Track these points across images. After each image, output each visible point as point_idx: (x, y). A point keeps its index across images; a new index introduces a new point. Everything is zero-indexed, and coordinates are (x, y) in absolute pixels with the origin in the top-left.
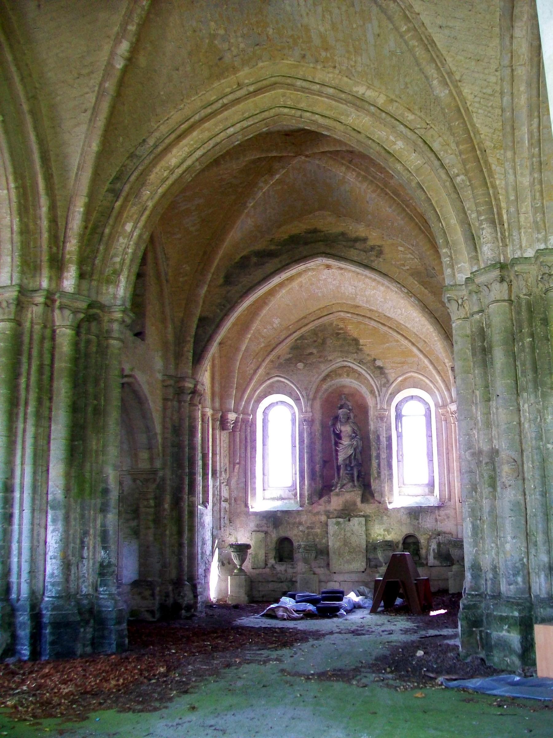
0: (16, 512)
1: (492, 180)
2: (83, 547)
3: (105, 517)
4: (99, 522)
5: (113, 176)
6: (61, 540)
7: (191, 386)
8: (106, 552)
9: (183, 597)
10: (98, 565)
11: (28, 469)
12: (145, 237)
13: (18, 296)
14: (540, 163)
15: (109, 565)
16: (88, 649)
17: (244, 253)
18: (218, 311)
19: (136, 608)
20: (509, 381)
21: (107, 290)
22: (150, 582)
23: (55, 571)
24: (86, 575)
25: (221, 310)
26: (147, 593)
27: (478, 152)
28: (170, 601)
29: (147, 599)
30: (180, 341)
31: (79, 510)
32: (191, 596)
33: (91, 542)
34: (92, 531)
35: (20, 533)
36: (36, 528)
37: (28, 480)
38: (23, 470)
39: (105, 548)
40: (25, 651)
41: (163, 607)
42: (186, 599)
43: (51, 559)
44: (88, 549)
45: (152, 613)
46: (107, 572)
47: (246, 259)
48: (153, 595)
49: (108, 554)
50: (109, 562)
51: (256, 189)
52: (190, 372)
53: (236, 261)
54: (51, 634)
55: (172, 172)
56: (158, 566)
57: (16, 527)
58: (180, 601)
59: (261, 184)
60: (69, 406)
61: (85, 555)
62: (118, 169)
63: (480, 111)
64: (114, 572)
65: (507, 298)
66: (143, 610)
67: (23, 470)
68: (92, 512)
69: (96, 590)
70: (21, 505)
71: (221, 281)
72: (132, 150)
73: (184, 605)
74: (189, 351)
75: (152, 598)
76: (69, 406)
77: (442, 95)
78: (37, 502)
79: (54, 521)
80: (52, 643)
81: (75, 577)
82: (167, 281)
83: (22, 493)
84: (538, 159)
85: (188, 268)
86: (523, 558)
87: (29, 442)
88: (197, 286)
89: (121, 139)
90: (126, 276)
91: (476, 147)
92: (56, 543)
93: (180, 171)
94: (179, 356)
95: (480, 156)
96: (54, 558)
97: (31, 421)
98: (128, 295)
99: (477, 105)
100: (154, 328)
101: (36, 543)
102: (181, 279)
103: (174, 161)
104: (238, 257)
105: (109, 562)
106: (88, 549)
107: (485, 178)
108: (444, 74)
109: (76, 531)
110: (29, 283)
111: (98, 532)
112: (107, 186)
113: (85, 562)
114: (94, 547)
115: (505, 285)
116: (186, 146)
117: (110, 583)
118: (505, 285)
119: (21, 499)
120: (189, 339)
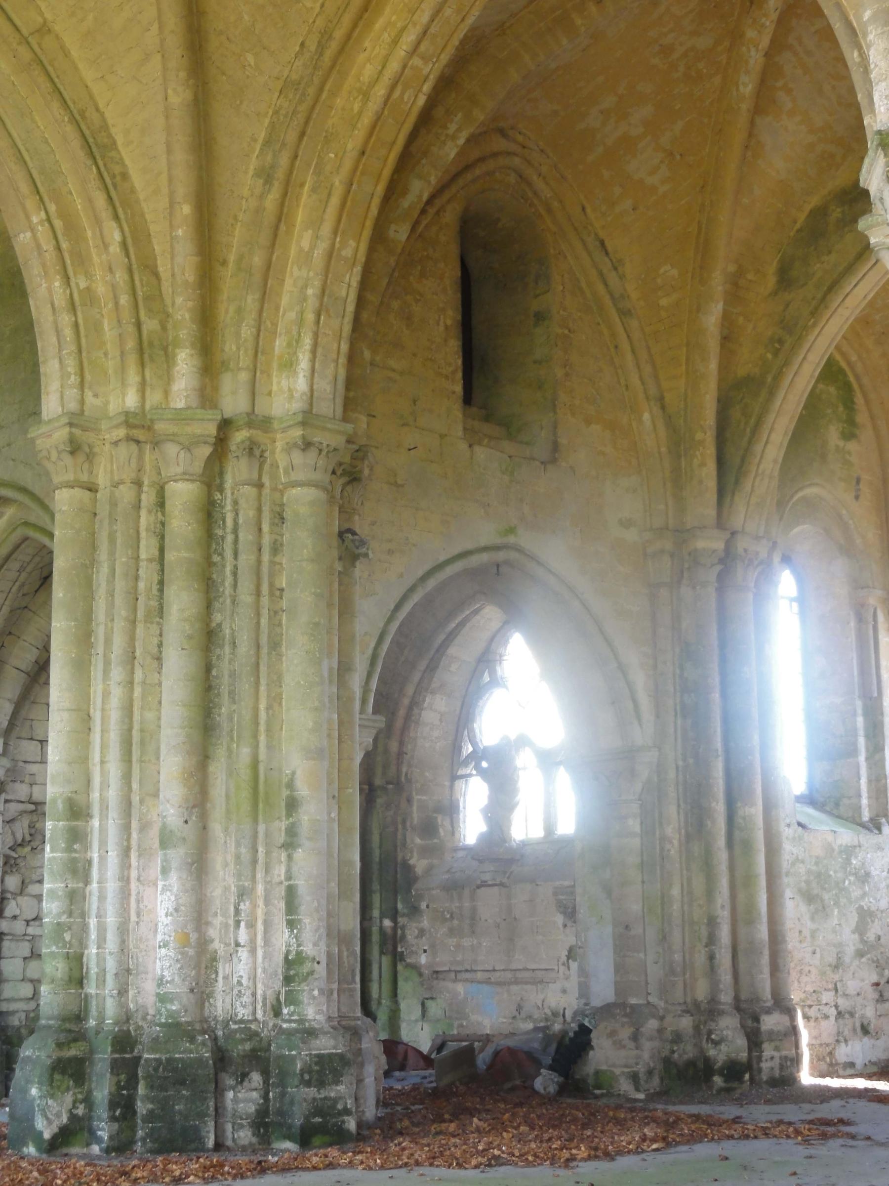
0: (95, 856)
2: (238, 923)
3: (290, 857)
4: (280, 871)
5: (260, 141)
6: (176, 910)
7: (720, 545)
8: (292, 931)
9: (716, 1043)
10: (279, 959)
11: (114, 770)
12: (348, 252)
13: (71, 433)
15: (300, 958)
16: (245, 1136)
17: (815, 201)
18: (769, 356)
19: (604, 1068)
21: (279, 383)
22: (632, 1007)
23: (166, 973)
24: (244, 981)
25: (776, 353)
26: (625, 1034)
28: (687, 1052)
29: (624, 1047)
30: (679, 445)
31: (232, 848)
32: (741, 1042)
33: (260, 913)
34: (260, 888)
35: (102, 898)
36: (134, 885)
37: (113, 794)
38: (104, 774)
39: (291, 924)
40: (104, 1131)
41: (667, 1062)
42: (723, 1047)
43: (160, 947)
44: (251, 925)
45: (634, 1078)
46: (296, 975)
47: (819, 213)
48: (635, 1037)
49: (296, 937)
50: (299, 953)
51: (744, 49)
52: (712, 512)
53: (798, 226)
54: (147, 1098)
55: (366, 96)
56: (655, 973)
57: (94, 886)
58: (712, 1053)
59: (750, 34)
60: (190, 637)
61: (243, 935)
62: (267, 121)
64: (312, 973)
66: (617, 1071)
67: (104, 774)
68: (261, 849)
69: (277, 1013)
70: (103, 843)
71: (772, 281)
72: (286, 74)
73: (719, 1064)
74: (703, 464)
75: (632, 1045)
76: (190, 637)
78: (135, 835)
79: (165, 871)
80: (151, 1117)
81: (225, 985)
82: (625, 313)
83: (103, 817)
85: (675, 272)
87: (115, 716)
88: (698, 310)
89: (250, 59)
90: (308, 347)
92: (167, 915)
93: (380, 91)
94: (678, 480)
96: (165, 946)
97: (117, 674)
98: (324, 385)
100: (596, 428)
101: (134, 918)
102: (664, 302)
103: (369, 71)
104: (802, 217)
105: (299, 953)
106: (251, 925)
109: (226, 889)
110: (108, 402)
111: (281, 891)
112: (253, 164)
113: (243, 954)
114: (267, 924)
116: (385, 29)
117: (305, 998)
119: (103, 830)
120: (699, 436)
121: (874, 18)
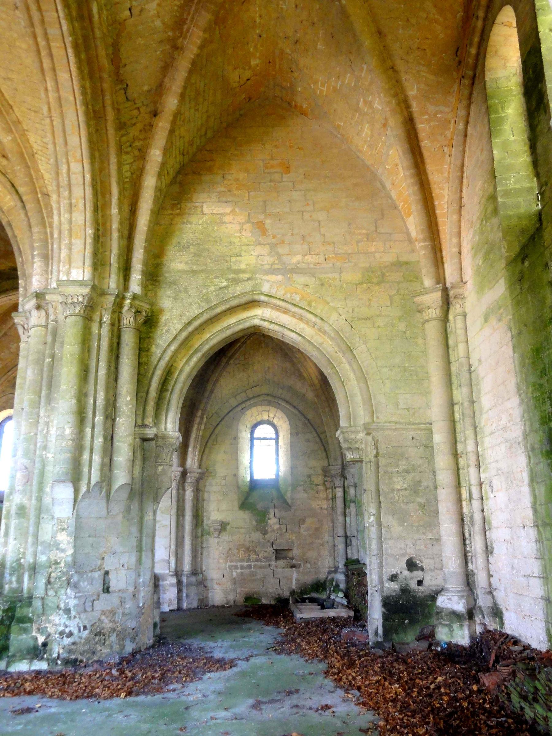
1: (50, 220)
14: (71, 204)
20: (33, 397)
27: (39, 195)
63: (43, 159)
65: (44, 324)
77: (5, 141)
84: (68, 201)
86: (21, 558)
91: (38, 190)
95: (41, 199)
99: (40, 153)
107: (43, 218)
108: (10, 122)
115: (43, 313)
118: (43, 313)
121: (38, 255)
